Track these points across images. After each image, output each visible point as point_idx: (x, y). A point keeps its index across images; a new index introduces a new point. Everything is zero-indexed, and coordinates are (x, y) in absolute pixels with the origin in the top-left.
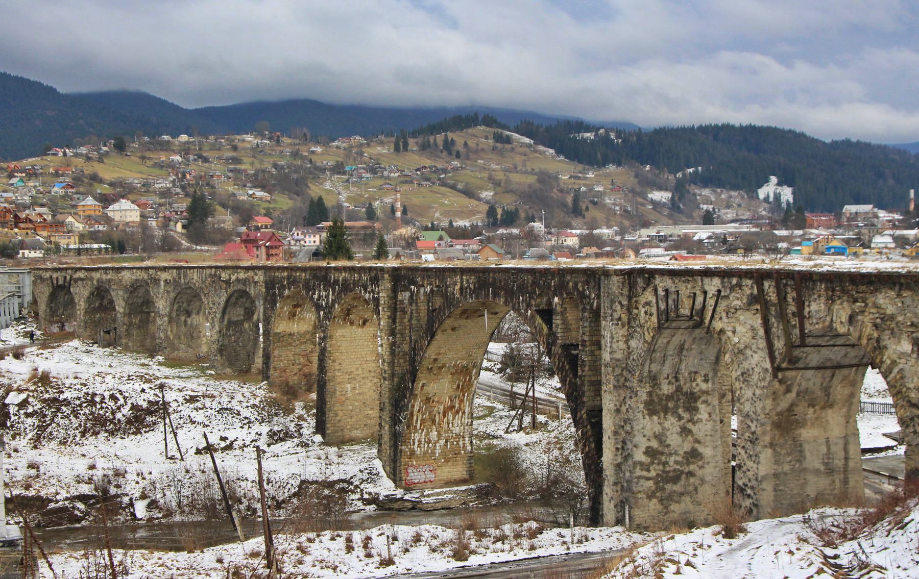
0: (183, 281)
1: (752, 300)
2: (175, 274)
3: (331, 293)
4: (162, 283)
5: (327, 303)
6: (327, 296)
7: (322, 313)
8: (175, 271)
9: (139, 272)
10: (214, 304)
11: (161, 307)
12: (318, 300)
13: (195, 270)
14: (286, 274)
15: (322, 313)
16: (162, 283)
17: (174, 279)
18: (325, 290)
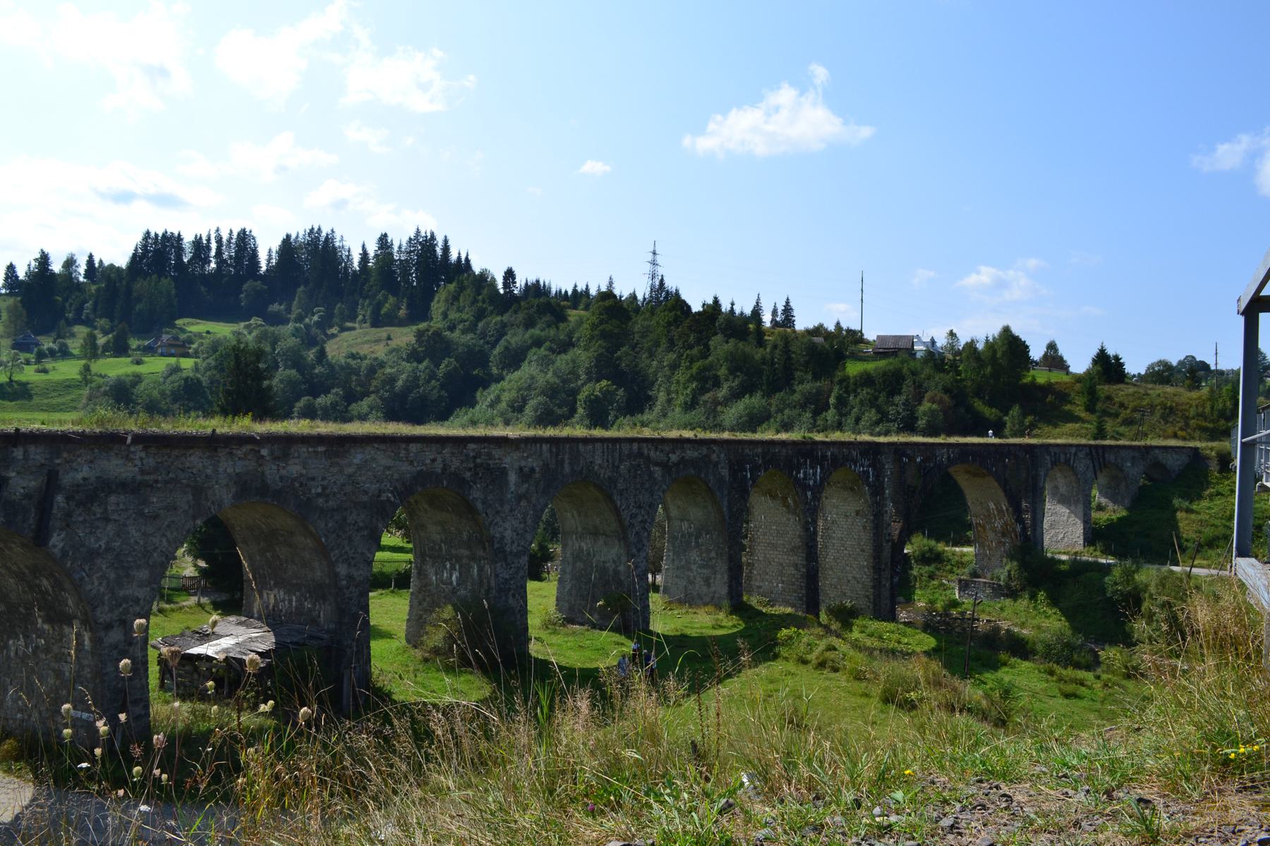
0: (567, 469)
1: (1087, 455)
2: (546, 455)
3: (819, 470)
4: (513, 478)
5: (815, 482)
6: (815, 474)
7: (809, 494)
8: (545, 447)
9: (429, 454)
10: (640, 507)
11: (508, 534)
12: (805, 478)
13: (598, 445)
14: (760, 450)
15: (809, 494)
16: (513, 478)
17: (546, 466)
18: (812, 467)
